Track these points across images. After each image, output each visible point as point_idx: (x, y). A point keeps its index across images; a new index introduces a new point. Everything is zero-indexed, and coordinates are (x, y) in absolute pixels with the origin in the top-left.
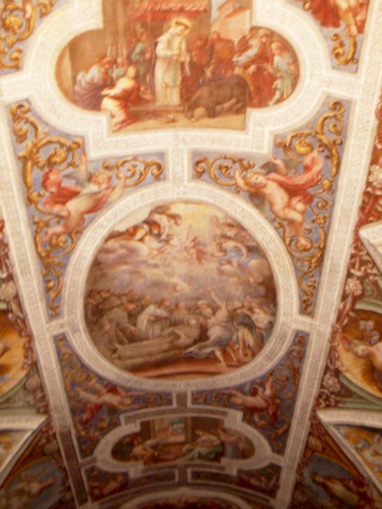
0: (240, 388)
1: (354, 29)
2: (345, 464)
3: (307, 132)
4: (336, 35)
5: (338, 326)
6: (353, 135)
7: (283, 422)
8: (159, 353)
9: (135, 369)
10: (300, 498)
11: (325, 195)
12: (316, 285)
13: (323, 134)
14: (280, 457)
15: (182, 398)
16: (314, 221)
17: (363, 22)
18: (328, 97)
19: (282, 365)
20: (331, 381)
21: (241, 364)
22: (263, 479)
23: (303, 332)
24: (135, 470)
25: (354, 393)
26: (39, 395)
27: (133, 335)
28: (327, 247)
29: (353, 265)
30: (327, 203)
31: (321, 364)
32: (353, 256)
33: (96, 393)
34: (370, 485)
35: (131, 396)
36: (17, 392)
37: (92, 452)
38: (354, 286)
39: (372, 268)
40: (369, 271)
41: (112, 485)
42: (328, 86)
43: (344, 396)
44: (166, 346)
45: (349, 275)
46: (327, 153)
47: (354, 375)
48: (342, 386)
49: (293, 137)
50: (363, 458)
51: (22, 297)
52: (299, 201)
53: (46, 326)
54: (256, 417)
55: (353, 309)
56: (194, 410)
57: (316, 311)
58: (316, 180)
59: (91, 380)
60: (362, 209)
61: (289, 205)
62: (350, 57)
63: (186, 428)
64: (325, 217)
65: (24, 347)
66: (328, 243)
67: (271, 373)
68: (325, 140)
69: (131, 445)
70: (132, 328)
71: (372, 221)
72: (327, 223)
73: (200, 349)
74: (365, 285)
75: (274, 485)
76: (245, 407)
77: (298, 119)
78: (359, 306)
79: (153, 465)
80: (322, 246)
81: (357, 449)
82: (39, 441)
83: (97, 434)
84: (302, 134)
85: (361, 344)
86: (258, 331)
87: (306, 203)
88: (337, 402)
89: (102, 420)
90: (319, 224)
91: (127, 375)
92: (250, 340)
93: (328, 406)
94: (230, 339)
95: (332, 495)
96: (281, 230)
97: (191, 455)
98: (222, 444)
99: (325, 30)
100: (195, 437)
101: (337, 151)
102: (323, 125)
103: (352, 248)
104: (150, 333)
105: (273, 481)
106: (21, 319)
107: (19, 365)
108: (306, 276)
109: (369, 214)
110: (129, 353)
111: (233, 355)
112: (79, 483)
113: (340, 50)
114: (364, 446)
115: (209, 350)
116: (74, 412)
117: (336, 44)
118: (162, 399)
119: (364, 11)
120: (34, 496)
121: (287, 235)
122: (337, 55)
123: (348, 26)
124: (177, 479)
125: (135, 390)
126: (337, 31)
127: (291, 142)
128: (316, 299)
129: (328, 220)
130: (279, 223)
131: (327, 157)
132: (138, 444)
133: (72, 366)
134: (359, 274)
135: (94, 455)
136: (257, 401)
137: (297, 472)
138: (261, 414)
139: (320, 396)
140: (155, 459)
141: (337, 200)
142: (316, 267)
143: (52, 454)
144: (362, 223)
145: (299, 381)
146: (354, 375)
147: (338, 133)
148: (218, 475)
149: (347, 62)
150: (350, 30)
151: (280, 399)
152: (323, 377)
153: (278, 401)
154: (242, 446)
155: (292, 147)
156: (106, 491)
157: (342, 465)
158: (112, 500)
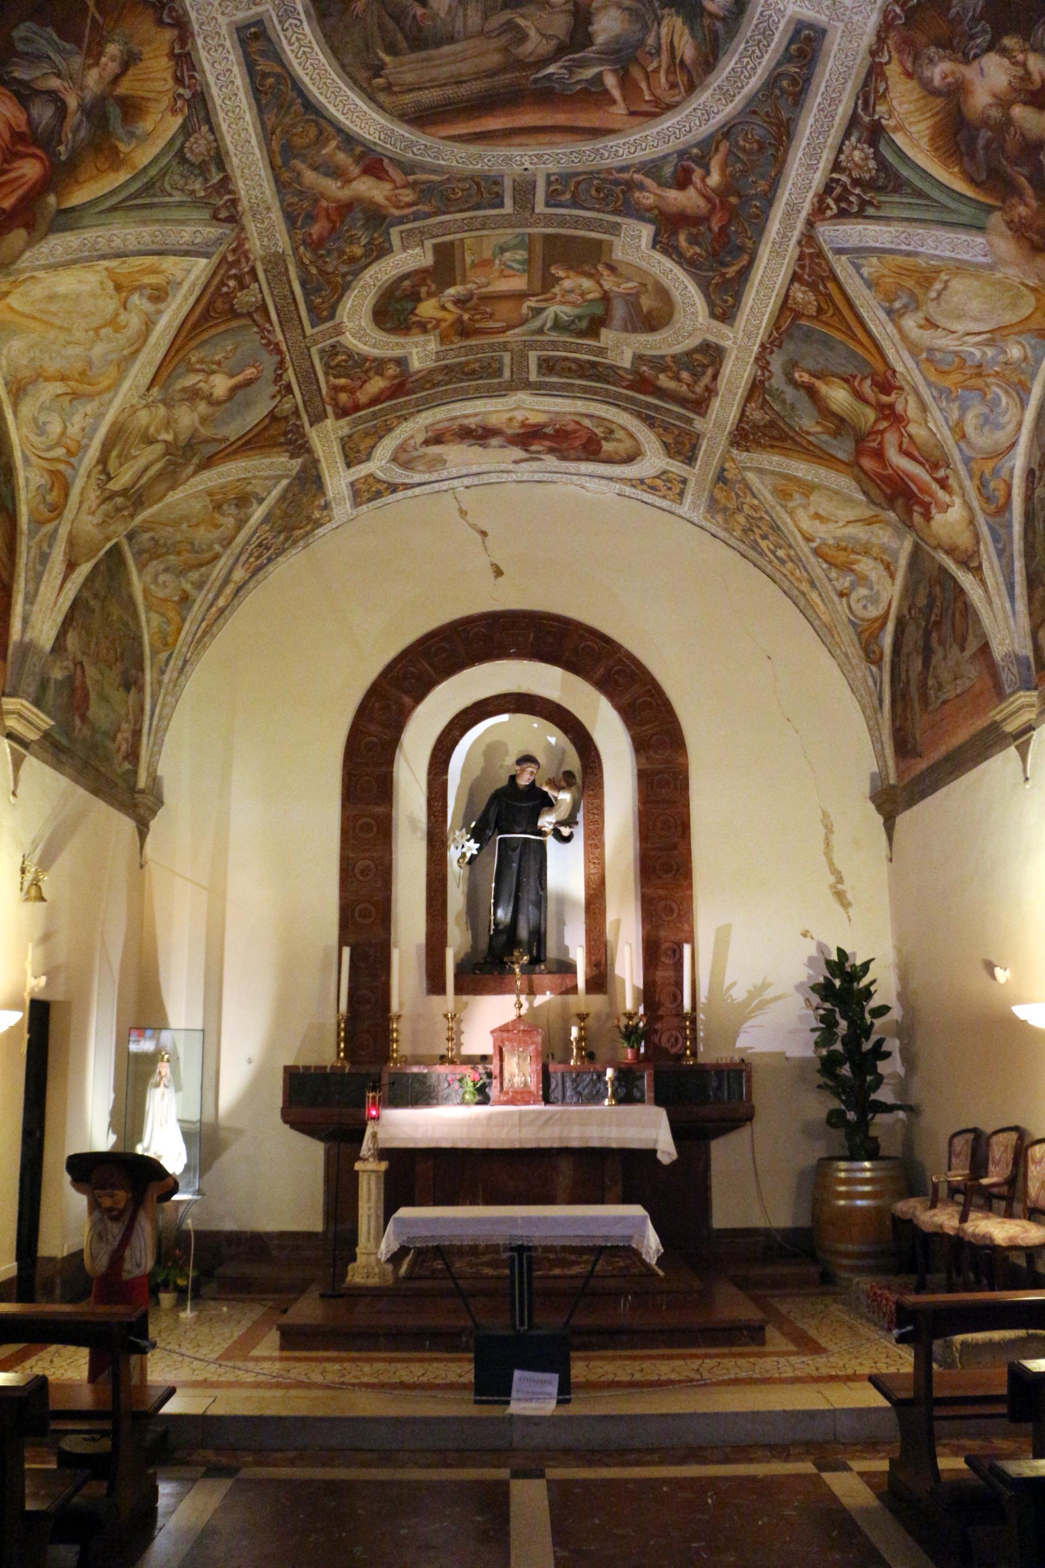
0: (652, 168)
2: (862, 344)
5: (898, 10)
7: (741, 249)
8: (478, 76)
9: (422, 118)
10: (756, 415)
14: (724, 329)
15: (524, 191)
19: (754, 112)
20: (858, 154)
21: (662, 108)
22: (685, 375)
23: (811, 26)
24: (421, 353)
25: (908, 183)
26: (216, 177)
27: (420, 30)
31: (843, 111)
33: (336, 173)
34: (907, 388)
35: (414, 185)
36: (168, 165)
37: (332, 316)
41: (377, 385)
43: (880, 190)
44: (495, 59)
47: (914, 138)
48: (883, 164)
50: (900, 330)
54: (682, 239)
56: (548, 220)
59: (325, 145)
63: (529, 262)
65: (172, 55)
67: (727, 131)
69: (416, 298)
70: (420, 11)
73: (570, 70)
75: (707, 388)
76: (661, 212)
79: (458, 343)
81: (889, 312)
82: (222, 283)
83: (344, 269)
85: (942, 59)
86: (707, 21)
88: (863, 204)
89: (352, 240)
91: (403, 131)
92: (687, 49)
93: (843, 214)
94: (641, 43)
95: (824, 411)
97: (536, 324)
98: (606, 298)
100: (549, 282)
104: (459, 24)
105: (705, 380)
107: (166, 101)
110: (409, 78)
111: (643, 85)
112: (308, 377)
114: (905, 306)
115: (589, 73)
116: (291, 219)
118: (484, 191)
120: (218, 403)
124: (507, 374)
125: (424, 168)
132: (430, 295)
133: (283, 107)
135: (337, 321)
136: (687, 200)
137: (757, 359)
138: (694, 231)
139: (828, 189)
140: (464, 331)
143: (249, 315)
145: (786, 151)
146: (914, 138)
148: (594, 365)
151: (740, 196)
152: (842, 143)
153: (733, 200)
154: (646, 303)
156: (362, 397)
157: (852, 344)
158: (375, 416)
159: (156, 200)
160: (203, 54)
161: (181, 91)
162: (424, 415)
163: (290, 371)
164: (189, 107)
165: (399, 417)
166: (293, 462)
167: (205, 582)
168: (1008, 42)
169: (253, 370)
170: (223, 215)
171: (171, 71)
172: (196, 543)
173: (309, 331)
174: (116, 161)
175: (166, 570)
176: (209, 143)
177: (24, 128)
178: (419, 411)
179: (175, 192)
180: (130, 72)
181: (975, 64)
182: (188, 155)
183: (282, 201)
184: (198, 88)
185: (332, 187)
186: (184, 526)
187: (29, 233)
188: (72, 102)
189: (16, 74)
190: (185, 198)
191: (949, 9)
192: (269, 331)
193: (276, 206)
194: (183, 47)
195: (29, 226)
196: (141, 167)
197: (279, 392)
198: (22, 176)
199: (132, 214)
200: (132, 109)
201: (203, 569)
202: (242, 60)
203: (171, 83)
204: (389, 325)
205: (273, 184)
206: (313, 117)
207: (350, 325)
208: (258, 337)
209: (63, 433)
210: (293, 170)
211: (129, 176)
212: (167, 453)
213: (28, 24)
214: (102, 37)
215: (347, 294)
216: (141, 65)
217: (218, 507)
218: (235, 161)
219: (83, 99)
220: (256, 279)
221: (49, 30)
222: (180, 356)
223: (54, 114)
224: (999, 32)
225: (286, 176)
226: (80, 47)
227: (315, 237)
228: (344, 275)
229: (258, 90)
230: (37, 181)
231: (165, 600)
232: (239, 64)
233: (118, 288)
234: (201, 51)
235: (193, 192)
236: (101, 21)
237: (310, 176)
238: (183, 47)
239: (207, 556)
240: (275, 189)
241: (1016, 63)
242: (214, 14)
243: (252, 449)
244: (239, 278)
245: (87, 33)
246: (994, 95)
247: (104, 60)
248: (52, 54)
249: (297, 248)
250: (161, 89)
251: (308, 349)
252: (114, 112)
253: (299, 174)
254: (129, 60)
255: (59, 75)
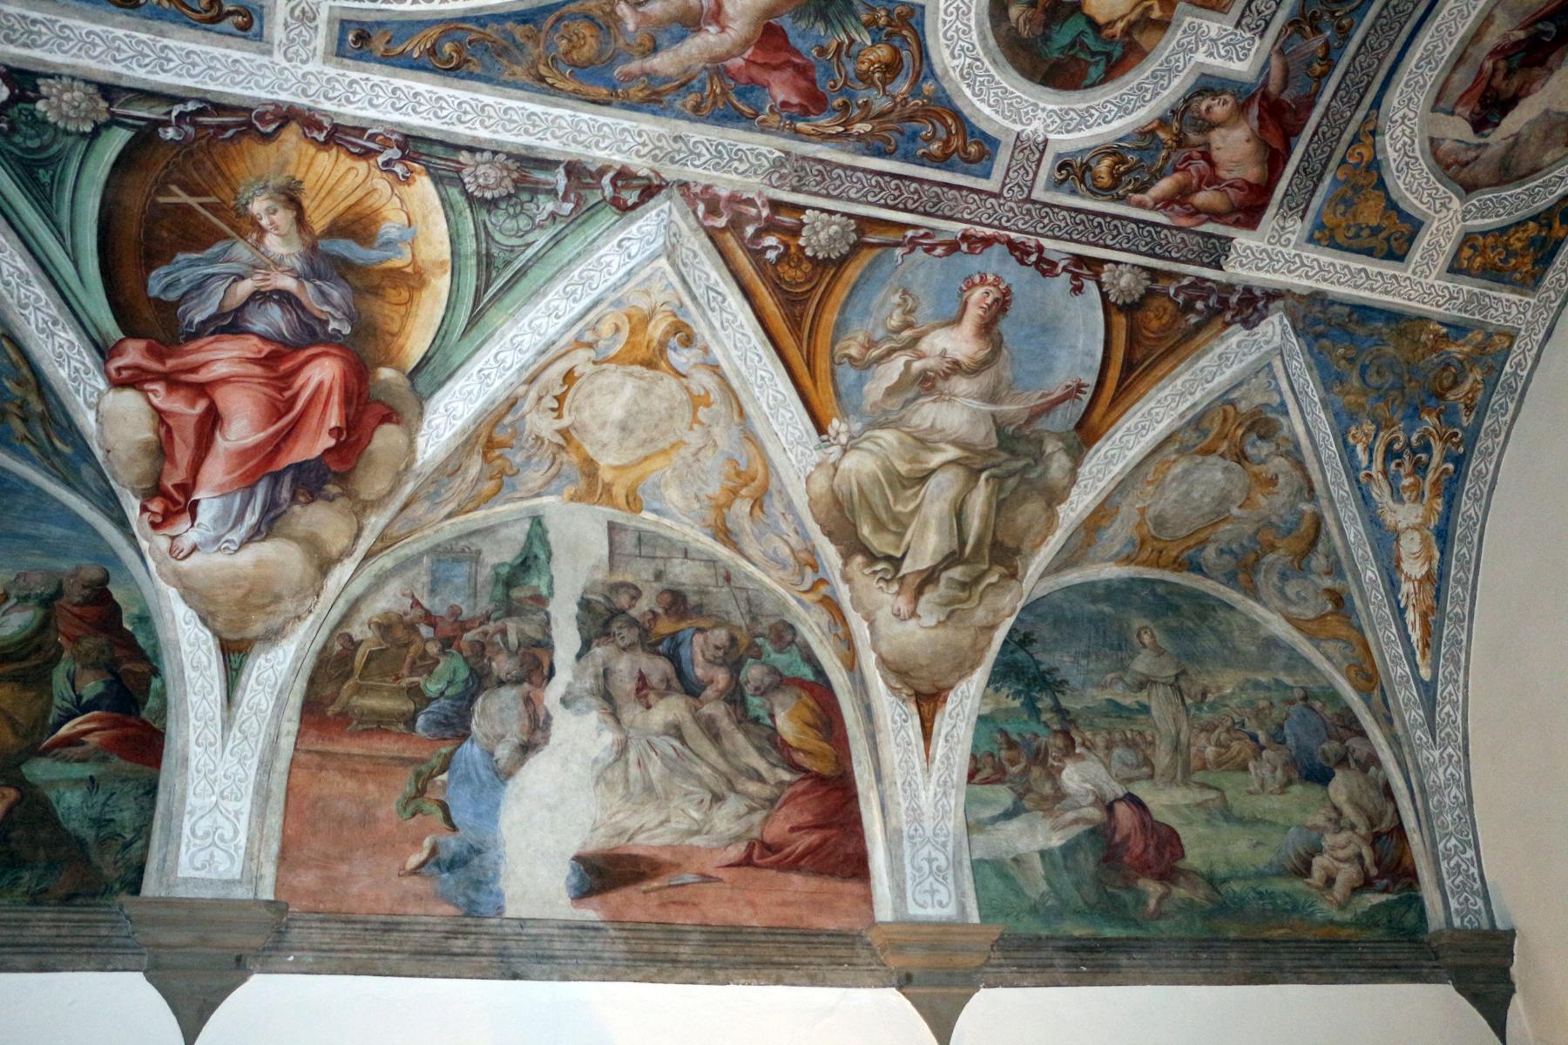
26: (560, 180)
37: (995, 143)
51: (118, 76)
53: (278, 57)
59: (619, 20)
65: (325, 145)
82: (757, 255)
83: (901, 86)
106: (200, 112)
107: (381, 184)
116: (728, 117)
143: (857, 247)
159: (517, 265)
160: (349, 110)
161: (381, 159)
162: (1394, 99)
163: (1045, 243)
164: (414, 160)
165: (1356, 139)
166: (1263, 327)
167: (1338, 561)
169: (978, 293)
170: (631, 197)
171: (342, 156)
172: (1274, 519)
173: (991, 185)
174: (412, 280)
175: (1283, 577)
176: (491, 162)
177: (267, 349)
178: (1377, 104)
179: (530, 238)
180: (306, 203)
182: (488, 195)
183: (680, 116)
184: (395, 137)
185: (710, 39)
186: (1235, 511)
187: (398, 423)
188: (288, 283)
189: (197, 319)
190: (551, 231)
192: (926, 236)
193: (683, 127)
194: (320, 128)
195: (390, 415)
196: (448, 257)
197: (1076, 276)
198: (320, 385)
199: (507, 300)
200: (357, 225)
201: (1320, 547)
202: (388, 69)
203: (362, 166)
204: (1094, 73)
205: (636, 115)
206: (551, 19)
207: (1036, 124)
208: (919, 253)
209: (792, 550)
210: (630, 77)
211: (448, 277)
212: (974, 474)
213: (153, 274)
214: (234, 209)
215: (959, 103)
216: (306, 185)
217: (1241, 457)
218: (552, 144)
219: (292, 270)
220: (800, 209)
221: (180, 257)
222: (822, 364)
223: (282, 308)
225: (636, 92)
226: (227, 237)
227: (795, 100)
228: (915, 90)
229: (454, 70)
230: (345, 375)
231: (1321, 618)
232: (395, 76)
233: (650, 364)
234: (342, 110)
235: (553, 216)
236: (213, 199)
237: (663, 62)
238: (320, 128)
239: (1306, 525)
240: (648, 116)
242: (300, 72)
243: (1153, 366)
244: (770, 227)
245: (215, 220)
247: (264, 222)
248: (210, 271)
249: (797, 131)
250: (359, 180)
251: (1028, 200)
252: (344, 248)
253: (647, 74)
254: (291, 197)
255: (241, 277)
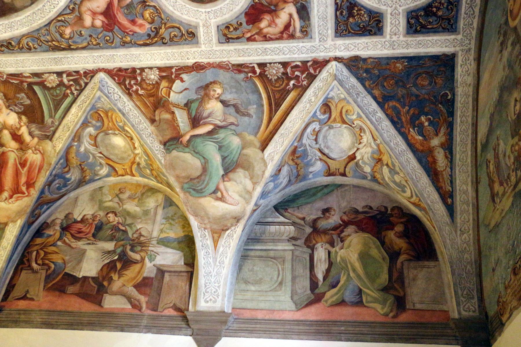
1: (249, 35)
3: (163, 16)
4: (241, 24)
5: (5, 77)
6: (174, 51)
11: (117, 41)
12: (33, 50)
13: (166, 29)
16: (91, 36)
17: (254, 40)
18: (196, 27)
28: (74, 52)
29: (69, 74)
30: (112, 42)
32: (77, 72)
38: (52, 80)
39: (76, 90)
40: (73, 88)
42: (204, 26)
45: (59, 74)
46: (153, 34)
49: (155, 7)
52: (103, 22)
55: (30, 85)
57: (6, 55)
58: (127, 31)
60: (120, 70)
61: (94, 14)
62: (229, 36)
64: (99, 44)
66: (79, 52)
68: (162, 31)
71: (114, 79)
72: (95, 47)
74: (59, 88)
77: (171, 8)
78: (36, 88)
80: (72, 47)
84: (160, 13)
87: (103, 26)
90: (91, 41)
96: (68, 11)
99: (243, 15)
101: (156, 42)
102: (173, 27)
103: (84, 71)
108: (36, 40)
109: (118, 76)
113: (232, 29)
117: (236, 25)
119: (261, 39)
121: (66, 17)
122: (227, 27)
123: (249, 31)
126: (244, 24)
127: (151, 6)
128: (18, 53)
129: (98, 47)
130: (73, 8)
131: (149, 35)
134: (65, 81)
141: (117, 50)
142: (50, 46)
144: (109, 72)
147: (171, 40)
149: (225, 35)
150: (247, 32)
155: (147, 7)
168: (23, 117)
181: (9, 111)
191: (19, 93)
224: (24, 113)
241: (19, 124)
246: (4, 122)
